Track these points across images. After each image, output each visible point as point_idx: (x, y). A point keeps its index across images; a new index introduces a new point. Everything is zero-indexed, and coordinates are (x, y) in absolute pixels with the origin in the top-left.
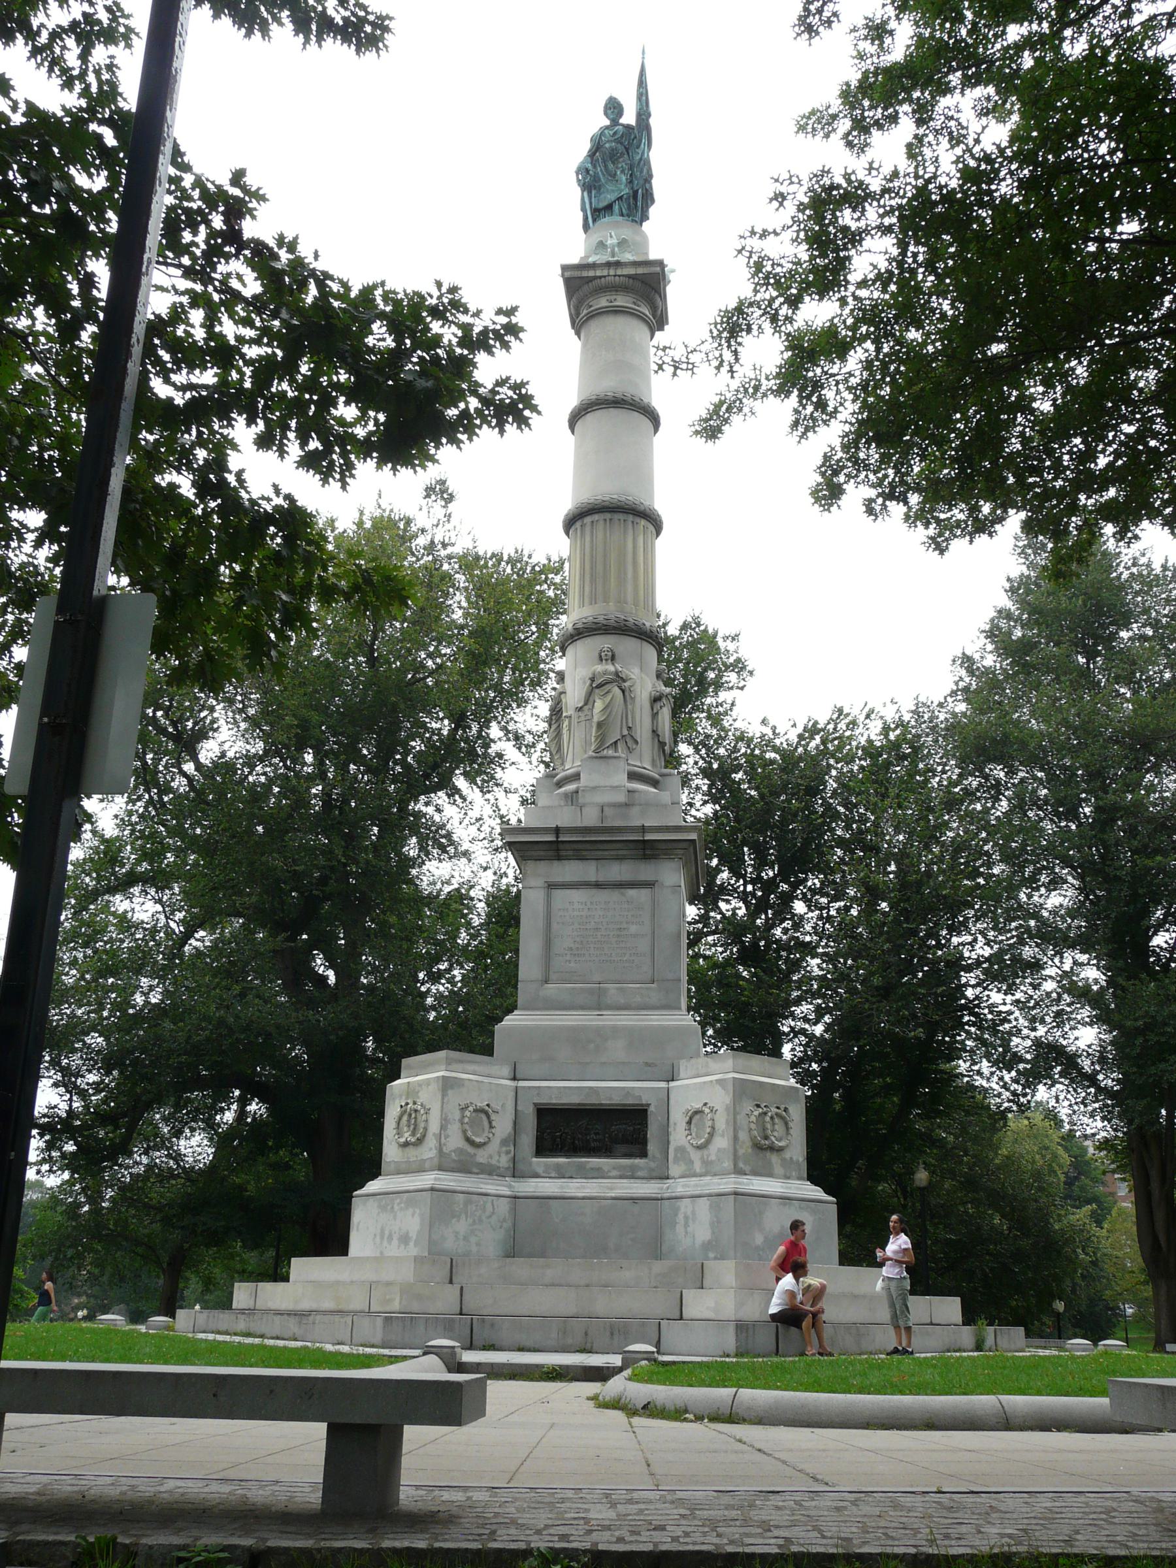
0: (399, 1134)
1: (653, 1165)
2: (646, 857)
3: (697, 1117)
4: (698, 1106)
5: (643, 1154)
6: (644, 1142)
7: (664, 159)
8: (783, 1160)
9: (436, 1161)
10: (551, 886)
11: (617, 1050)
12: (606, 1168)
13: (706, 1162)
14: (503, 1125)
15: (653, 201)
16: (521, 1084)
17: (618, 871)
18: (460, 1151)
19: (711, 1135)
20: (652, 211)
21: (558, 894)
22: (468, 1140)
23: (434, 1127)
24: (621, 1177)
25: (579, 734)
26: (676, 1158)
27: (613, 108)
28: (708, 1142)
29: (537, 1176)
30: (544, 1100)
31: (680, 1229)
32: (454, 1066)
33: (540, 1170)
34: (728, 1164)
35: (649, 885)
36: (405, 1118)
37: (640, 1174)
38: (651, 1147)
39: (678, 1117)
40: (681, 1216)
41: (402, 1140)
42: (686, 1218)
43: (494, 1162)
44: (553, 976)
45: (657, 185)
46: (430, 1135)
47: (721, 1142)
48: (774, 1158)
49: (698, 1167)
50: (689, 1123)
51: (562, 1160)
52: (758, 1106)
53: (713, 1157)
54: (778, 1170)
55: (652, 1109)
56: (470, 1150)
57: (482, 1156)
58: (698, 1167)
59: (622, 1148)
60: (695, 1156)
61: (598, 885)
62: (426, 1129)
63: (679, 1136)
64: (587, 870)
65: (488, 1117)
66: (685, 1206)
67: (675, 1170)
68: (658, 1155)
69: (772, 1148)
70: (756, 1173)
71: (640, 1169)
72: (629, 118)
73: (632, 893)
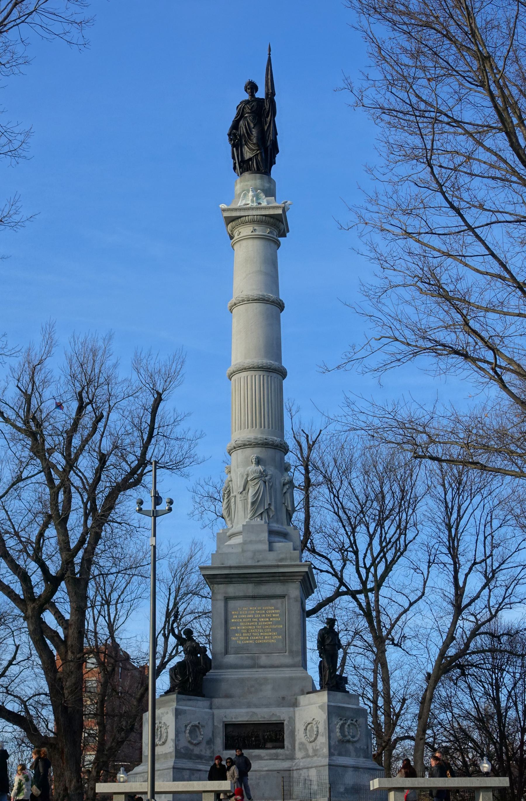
1: (287, 752)
3: (310, 726)
4: (310, 720)
5: (283, 747)
7: (284, 121)
8: (356, 748)
9: (174, 754)
11: (268, 692)
12: (263, 755)
16: (216, 712)
17: (264, 589)
18: (186, 748)
19: (317, 735)
20: (278, 157)
21: (232, 604)
22: (189, 742)
24: (271, 759)
26: (300, 749)
27: (252, 87)
28: (315, 739)
30: (228, 720)
32: (180, 703)
34: (326, 751)
35: (283, 597)
37: (280, 757)
38: (286, 743)
39: (300, 727)
43: (203, 753)
46: (169, 740)
47: (323, 740)
48: (350, 747)
49: (311, 752)
50: (306, 729)
52: (341, 719)
53: (318, 747)
54: (353, 753)
55: (285, 723)
56: (191, 747)
57: (197, 751)
58: (311, 752)
60: (310, 747)
61: (254, 597)
62: (167, 736)
63: (300, 736)
64: (249, 589)
65: (199, 729)
67: (299, 754)
68: (290, 747)
69: (348, 741)
70: (340, 754)
73: (273, 601)
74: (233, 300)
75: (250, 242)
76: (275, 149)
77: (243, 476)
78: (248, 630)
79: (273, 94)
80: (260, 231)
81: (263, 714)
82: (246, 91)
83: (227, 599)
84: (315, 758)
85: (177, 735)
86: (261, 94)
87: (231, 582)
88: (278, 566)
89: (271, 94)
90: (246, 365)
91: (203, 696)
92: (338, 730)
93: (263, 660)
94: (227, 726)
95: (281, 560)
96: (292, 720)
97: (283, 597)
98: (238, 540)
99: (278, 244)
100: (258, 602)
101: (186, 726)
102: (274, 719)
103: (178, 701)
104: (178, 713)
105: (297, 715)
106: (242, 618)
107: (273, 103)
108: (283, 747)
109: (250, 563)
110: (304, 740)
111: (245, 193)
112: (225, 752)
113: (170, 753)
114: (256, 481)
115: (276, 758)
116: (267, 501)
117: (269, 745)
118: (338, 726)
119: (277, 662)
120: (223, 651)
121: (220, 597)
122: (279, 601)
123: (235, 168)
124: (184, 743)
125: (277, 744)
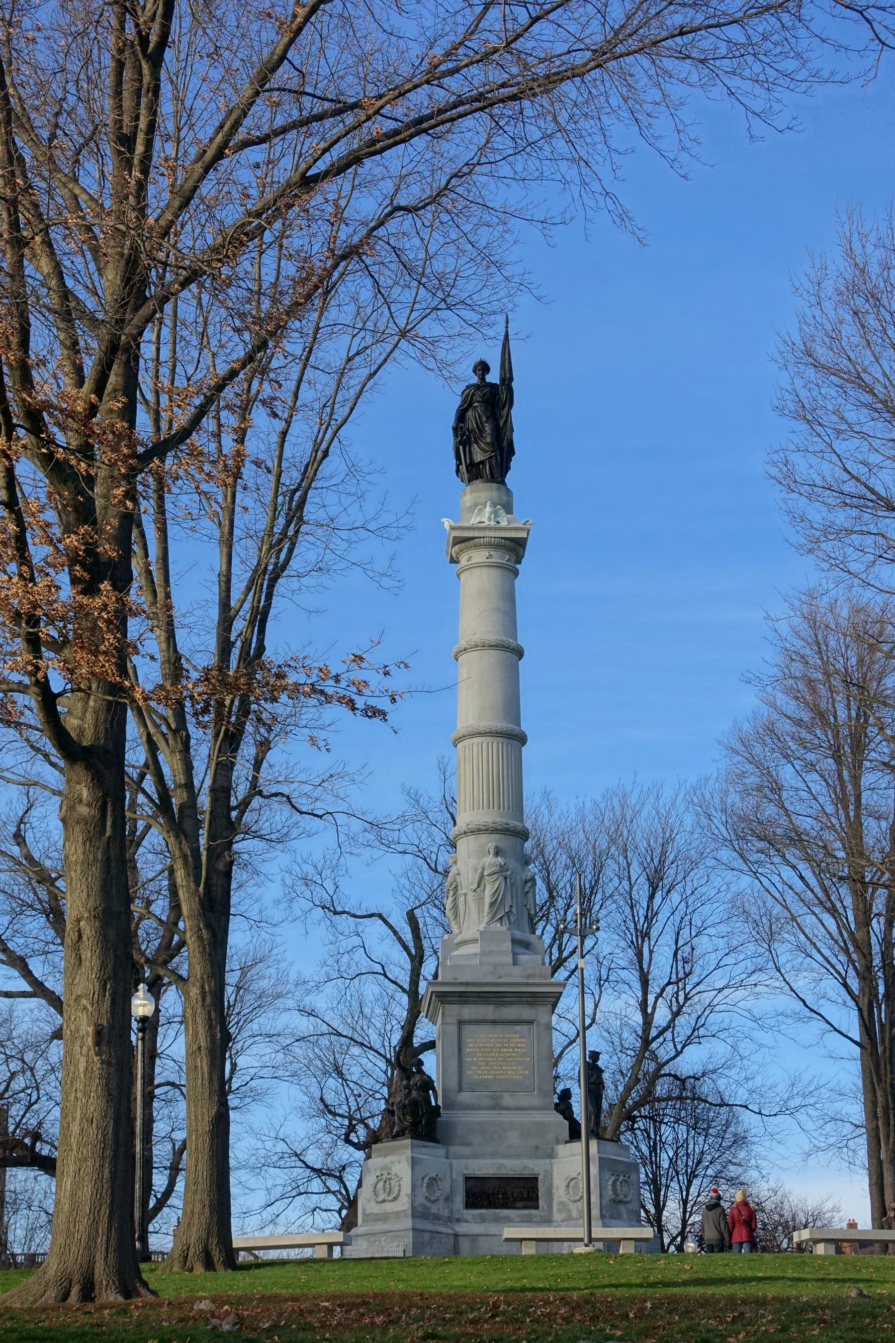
0: (376, 1194)
2: (529, 1003)
5: (537, 1207)
7: (522, 417)
9: (410, 1212)
10: (461, 1023)
11: (513, 1138)
14: (445, 1186)
15: (514, 453)
16: (455, 1162)
18: (423, 1205)
21: (467, 1028)
22: (426, 1198)
23: (406, 1188)
25: (473, 907)
27: (483, 368)
29: (467, 1221)
33: (469, 1218)
35: (531, 1022)
36: (381, 1184)
38: (541, 1202)
41: (381, 1199)
44: (464, 1086)
45: (518, 439)
46: (403, 1194)
48: (622, 1209)
50: (568, 1186)
51: (484, 1211)
56: (428, 1204)
57: (434, 1209)
61: (494, 1022)
62: (399, 1191)
63: (560, 1193)
64: (488, 1011)
67: (557, 1216)
69: (621, 1202)
71: (535, 1216)
72: (493, 377)
73: (518, 1028)
74: (463, 643)
75: (485, 572)
76: (511, 451)
77: (476, 870)
78: (487, 1062)
79: (511, 379)
80: (498, 557)
81: (513, 1166)
82: (474, 371)
83: (461, 1023)
85: (413, 1190)
87: (466, 1003)
88: (527, 984)
89: (507, 379)
90: (481, 729)
91: (437, 1142)
92: (610, 1187)
93: (507, 1100)
94: (467, 1179)
95: (528, 977)
96: (549, 1174)
97: (531, 1022)
98: (474, 949)
99: (516, 573)
100: (499, 1028)
101: (423, 1178)
102: (526, 1173)
103: (413, 1147)
104: (414, 1162)
105: (555, 1169)
106: (480, 1048)
107: (510, 391)
108: (537, 1207)
109: (489, 979)
110: (564, 1199)
111: (476, 507)
112: (466, 1211)
113: (405, 1211)
114: (495, 876)
115: (528, 1221)
116: (508, 903)
117: (519, 1204)
118: (610, 1183)
119: (524, 1103)
120: (456, 1087)
121: (452, 1020)
122: (525, 1027)
123: (458, 471)
124: (421, 1200)
125: (531, 1204)
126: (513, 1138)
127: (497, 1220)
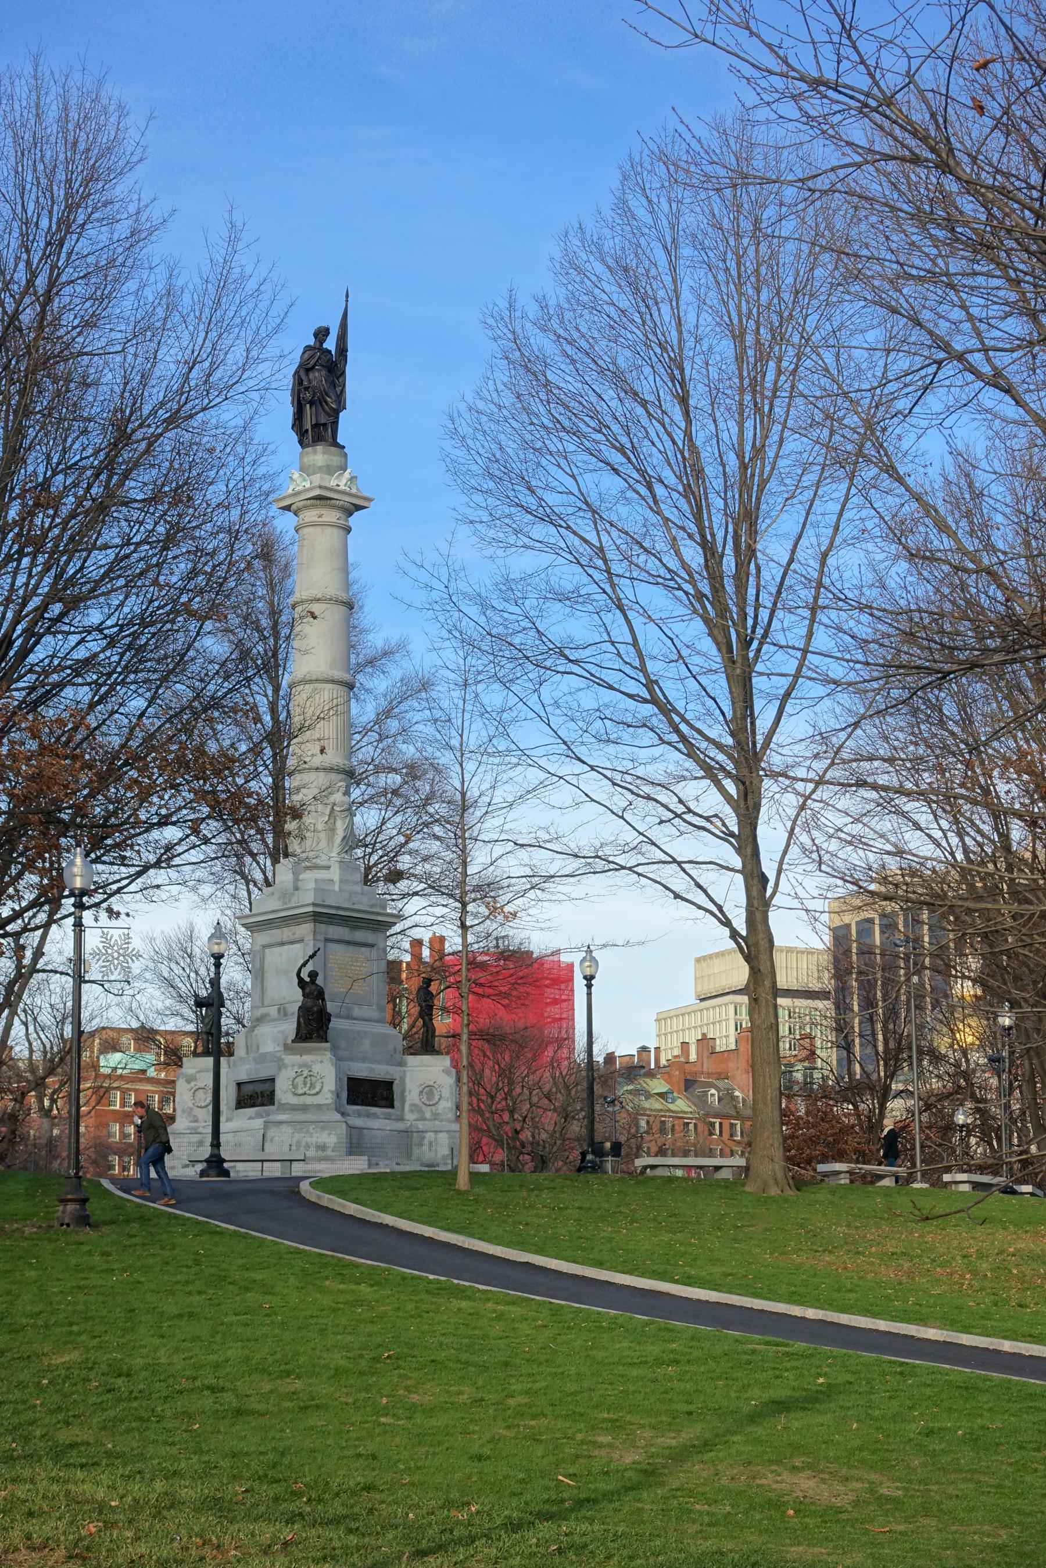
0: (295, 1086)
5: (392, 1106)
6: (392, 1100)
11: (366, 1044)
13: (433, 1114)
17: (360, 936)
31: (425, 1148)
34: (451, 1116)
35: (372, 946)
38: (397, 1103)
40: (426, 1141)
41: (300, 1091)
42: (431, 1143)
46: (325, 1089)
58: (428, 1115)
59: (383, 1103)
61: (348, 943)
66: (430, 1136)
72: (330, 344)
73: (363, 949)
75: (335, 530)
81: (379, 1071)
84: (437, 1123)
86: (330, 344)
87: (331, 923)
93: (356, 1012)
95: (372, 906)
96: (403, 1080)
97: (372, 946)
100: (351, 948)
102: (388, 1078)
105: (408, 1075)
108: (392, 1106)
109: (345, 905)
110: (417, 1102)
115: (388, 1117)
126: (366, 1044)
127: (368, 1115)
